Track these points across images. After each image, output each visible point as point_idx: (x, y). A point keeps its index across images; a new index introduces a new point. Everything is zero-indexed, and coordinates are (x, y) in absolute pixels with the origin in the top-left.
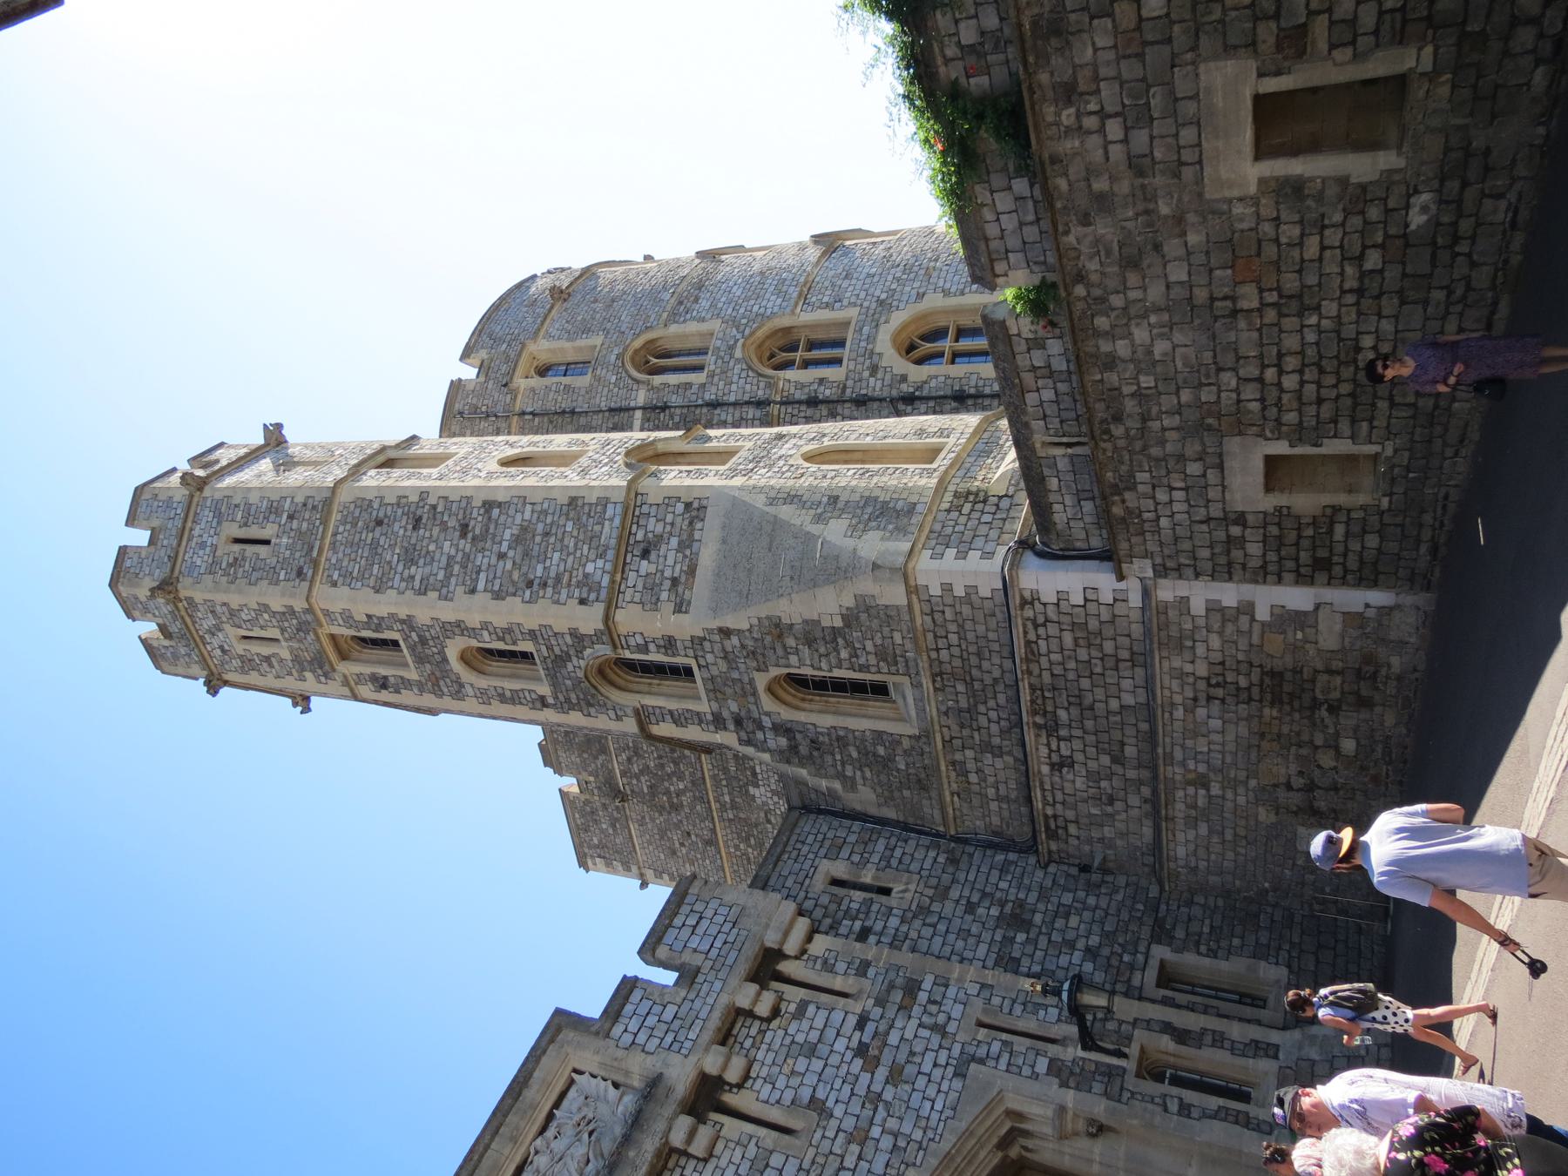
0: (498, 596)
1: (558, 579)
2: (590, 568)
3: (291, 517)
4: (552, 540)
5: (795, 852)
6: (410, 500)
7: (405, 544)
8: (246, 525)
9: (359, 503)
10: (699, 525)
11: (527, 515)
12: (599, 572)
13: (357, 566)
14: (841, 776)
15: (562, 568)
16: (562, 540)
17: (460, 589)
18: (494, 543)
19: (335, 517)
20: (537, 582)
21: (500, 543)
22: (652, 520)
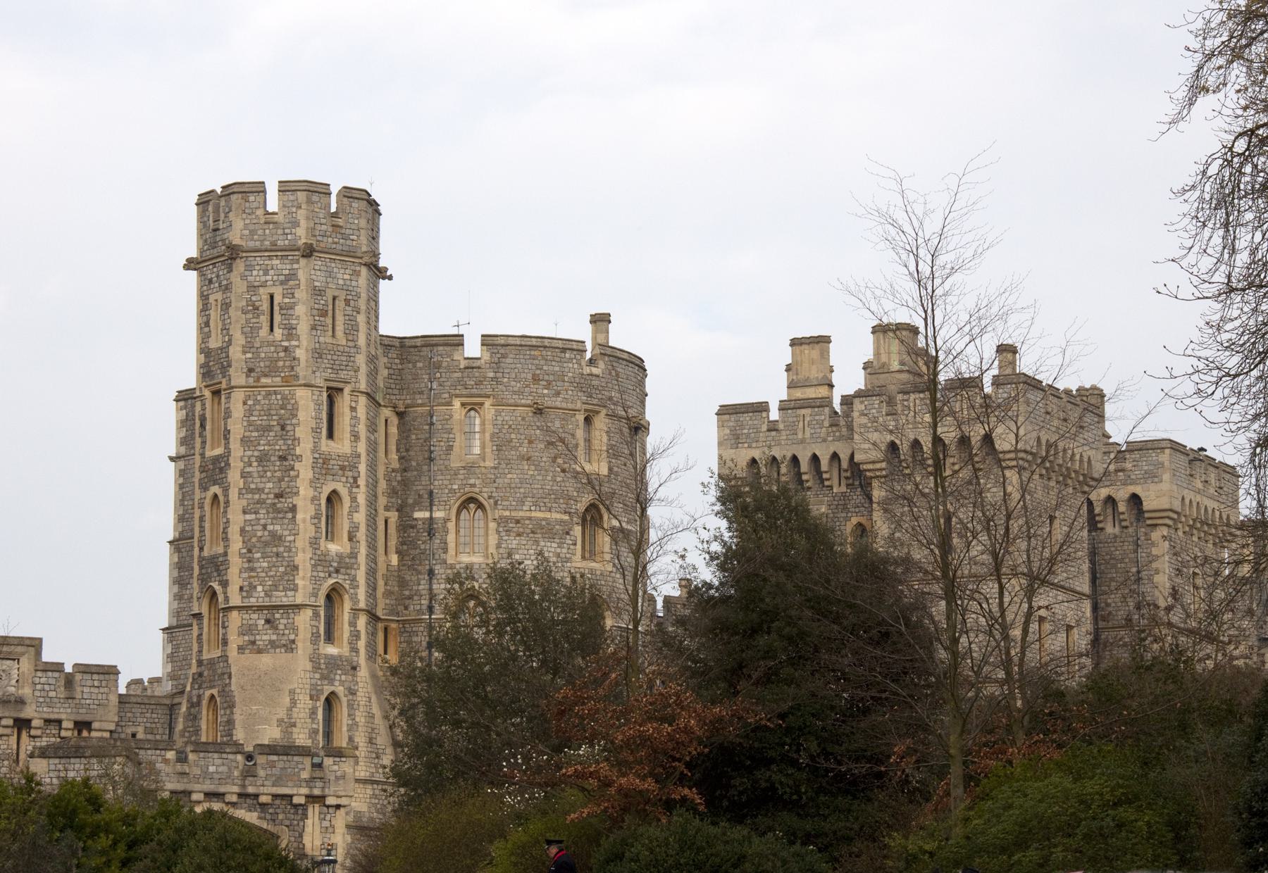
0: (243, 531)
1: (252, 569)
2: (260, 588)
3: (286, 349)
4: (274, 559)
5: (145, 711)
6: (297, 448)
7: (271, 452)
8: (281, 308)
9: (295, 406)
10: (283, 650)
11: (289, 538)
12: (257, 595)
13: (256, 419)
14: (184, 730)
15: (259, 570)
16: (274, 566)
17: (244, 503)
18: (272, 519)
19: (286, 390)
20: (250, 555)
21: (272, 524)
22: (285, 621)
